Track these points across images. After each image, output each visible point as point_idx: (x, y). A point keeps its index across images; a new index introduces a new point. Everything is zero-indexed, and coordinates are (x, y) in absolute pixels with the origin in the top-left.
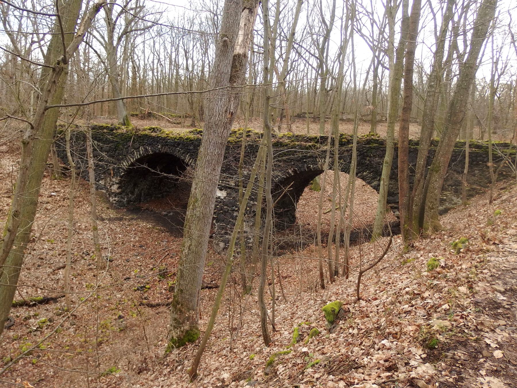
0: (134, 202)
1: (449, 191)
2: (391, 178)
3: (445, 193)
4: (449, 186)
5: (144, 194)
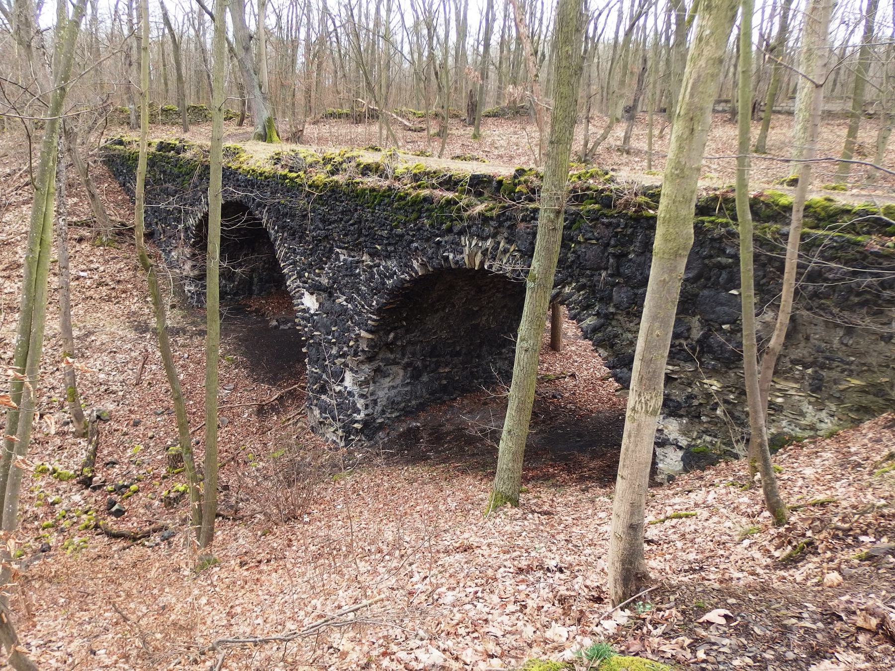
0: (235, 294)
1: (796, 381)
2: (688, 304)
3: (782, 384)
4: (795, 362)
5: (260, 280)
